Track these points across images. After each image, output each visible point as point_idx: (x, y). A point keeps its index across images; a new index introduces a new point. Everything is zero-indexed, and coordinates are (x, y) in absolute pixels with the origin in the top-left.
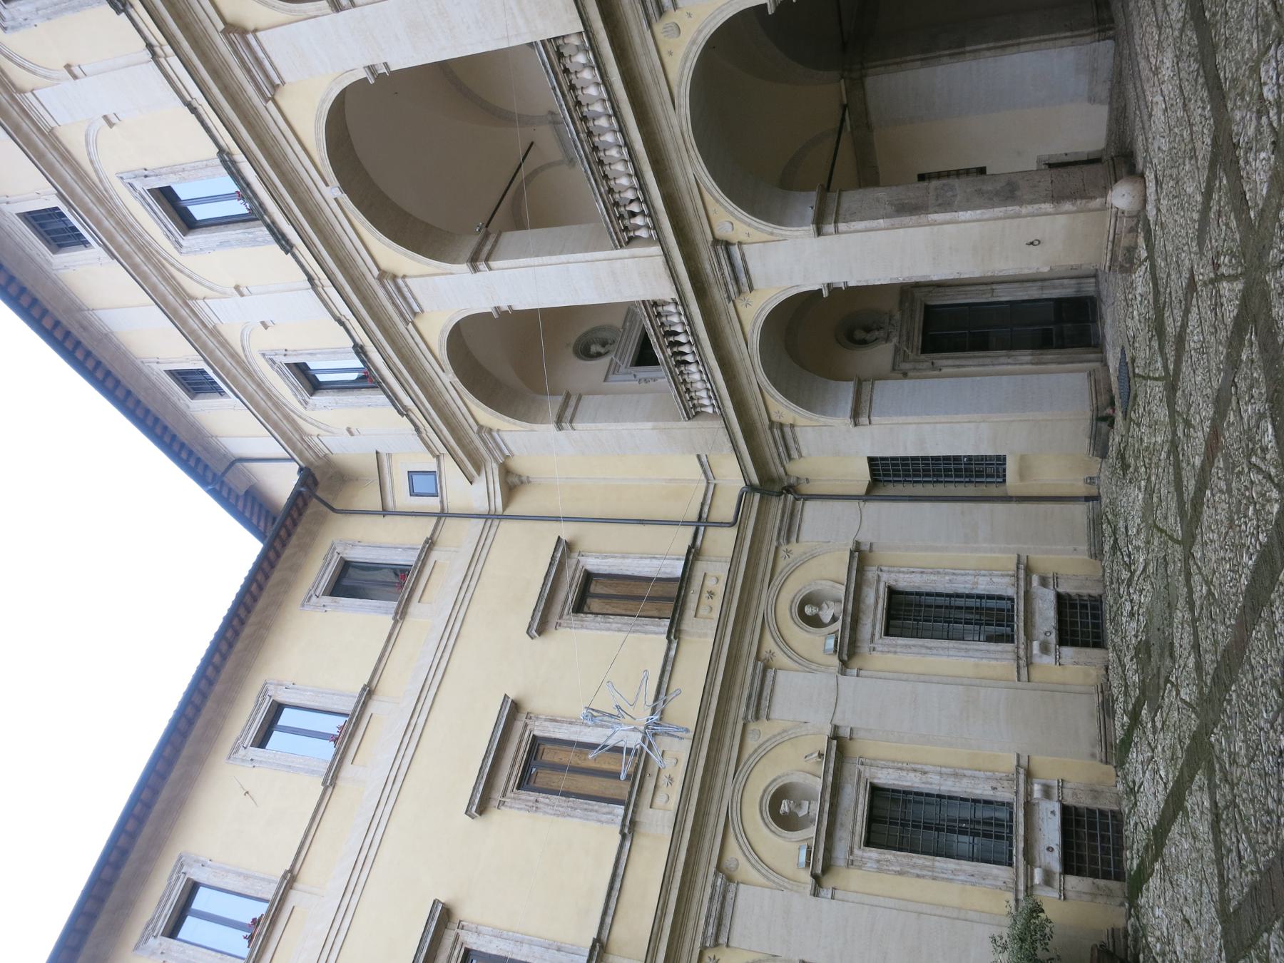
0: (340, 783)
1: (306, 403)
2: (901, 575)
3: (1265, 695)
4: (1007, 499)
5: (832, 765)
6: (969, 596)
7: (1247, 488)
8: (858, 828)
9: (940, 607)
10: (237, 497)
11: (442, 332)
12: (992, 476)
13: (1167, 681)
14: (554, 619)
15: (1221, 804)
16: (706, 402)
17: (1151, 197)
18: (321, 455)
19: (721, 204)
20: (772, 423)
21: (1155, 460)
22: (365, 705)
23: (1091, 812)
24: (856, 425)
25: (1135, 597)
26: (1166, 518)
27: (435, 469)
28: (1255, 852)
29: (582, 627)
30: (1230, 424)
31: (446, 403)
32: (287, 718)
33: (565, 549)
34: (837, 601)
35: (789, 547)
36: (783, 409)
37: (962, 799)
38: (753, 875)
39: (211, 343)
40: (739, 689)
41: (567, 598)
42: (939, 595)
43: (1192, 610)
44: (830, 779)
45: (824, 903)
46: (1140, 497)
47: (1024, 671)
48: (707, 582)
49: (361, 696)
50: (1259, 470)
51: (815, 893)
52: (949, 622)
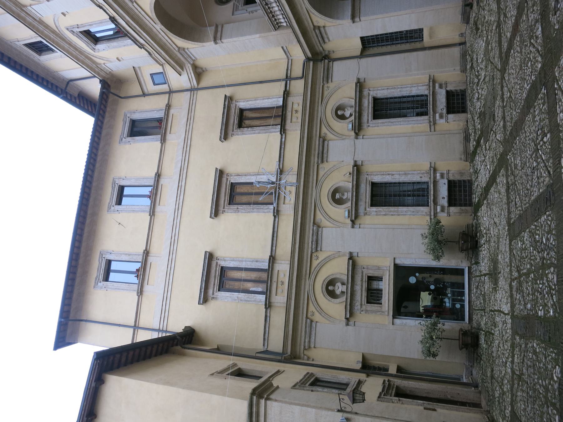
0: (156, 214)
1: (94, 49)
2: (379, 91)
3: (529, 144)
4: (424, 49)
5: (355, 177)
6: (409, 97)
7: (528, 54)
8: (367, 200)
9: (396, 103)
10: (75, 98)
11: (150, 4)
12: (417, 38)
13: (492, 130)
14: (230, 132)
15: (510, 183)
16: (282, 20)
18: (108, 72)
21: (490, 29)
22: (158, 181)
23: (460, 181)
24: (354, 22)
25: (480, 91)
26: (494, 58)
27: (162, 71)
28: (521, 203)
29: (243, 134)
30: (523, 21)
31: (160, 39)
32: (127, 191)
33: (229, 100)
34: (352, 107)
35: (328, 85)
36: (319, 19)
37: (408, 183)
38: (327, 223)
39: (41, 28)
40: (314, 151)
41: (234, 122)
42: (395, 98)
43: (503, 102)
44: (355, 183)
45: (356, 230)
46: (484, 45)
47: (432, 127)
48: (294, 106)
49: (155, 177)
50: (534, 47)
51: (353, 227)
52: (400, 110)
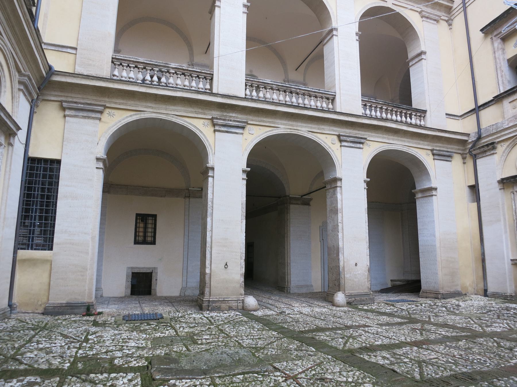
17: (342, 309)
19: (264, 133)
20: (106, 107)
